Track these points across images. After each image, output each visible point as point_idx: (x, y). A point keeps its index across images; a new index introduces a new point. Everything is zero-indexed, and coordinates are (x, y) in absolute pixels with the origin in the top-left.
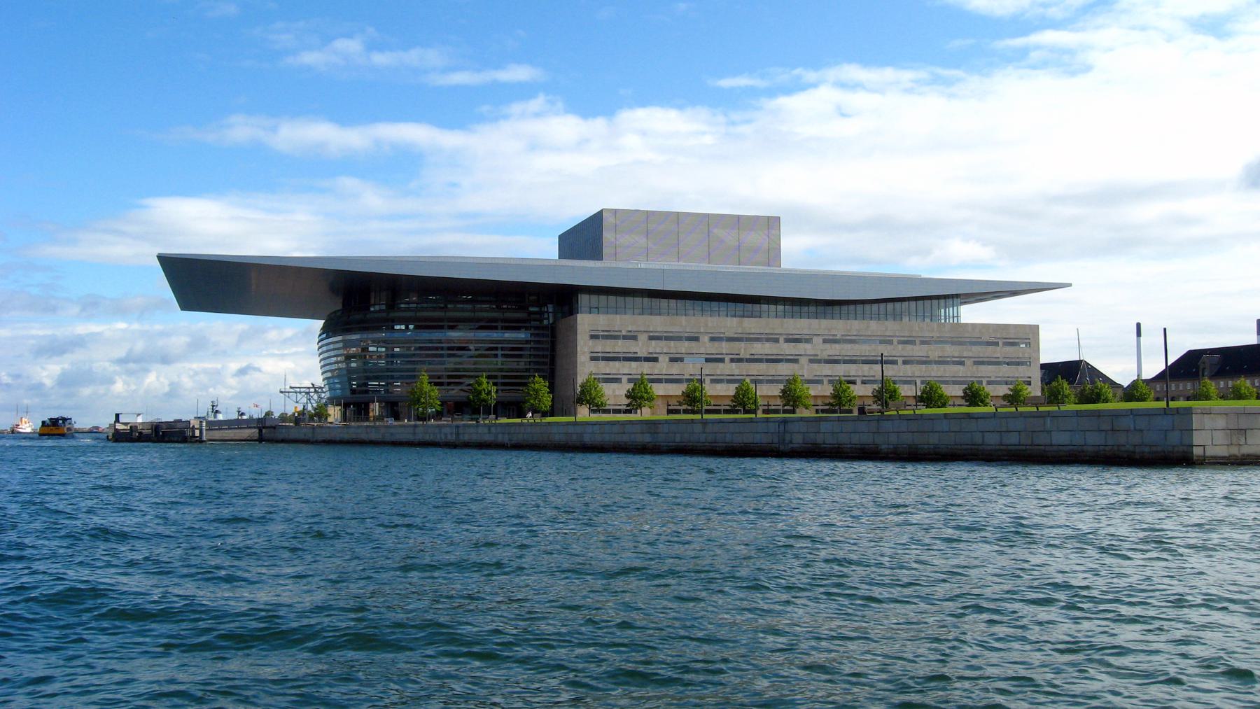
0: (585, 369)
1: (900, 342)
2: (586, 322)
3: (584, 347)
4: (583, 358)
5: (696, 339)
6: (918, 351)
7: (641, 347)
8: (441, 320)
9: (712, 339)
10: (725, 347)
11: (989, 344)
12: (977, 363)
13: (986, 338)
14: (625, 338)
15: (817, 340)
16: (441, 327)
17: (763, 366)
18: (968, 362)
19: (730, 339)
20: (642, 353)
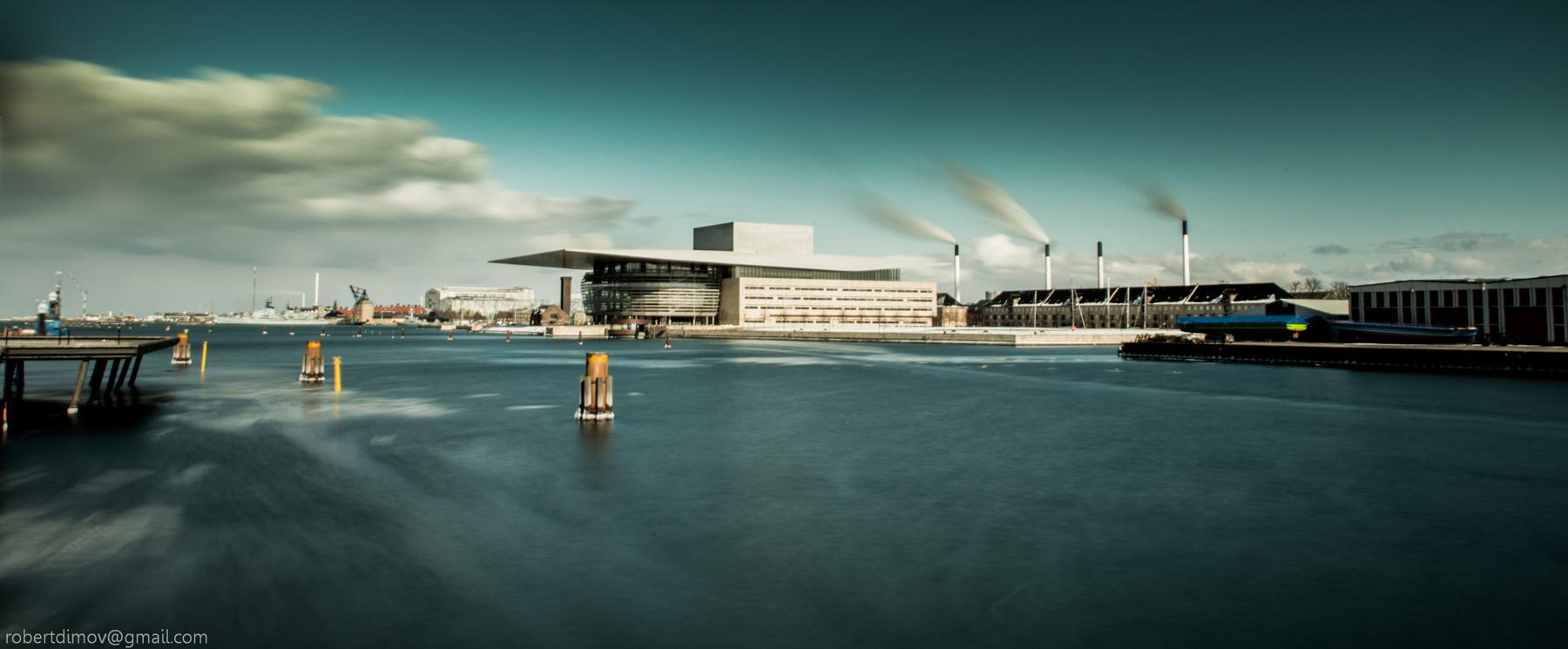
0: (743, 302)
1: (876, 291)
2: (744, 282)
3: (743, 292)
4: (742, 298)
5: (789, 289)
6: (883, 295)
7: (766, 293)
8: (668, 278)
9: (797, 289)
10: (801, 293)
11: (915, 291)
12: (909, 301)
13: (913, 289)
14: (760, 288)
15: (840, 290)
16: (668, 281)
17: (817, 301)
18: (905, 300)
19: (803, 289)
20: (767, 296)
